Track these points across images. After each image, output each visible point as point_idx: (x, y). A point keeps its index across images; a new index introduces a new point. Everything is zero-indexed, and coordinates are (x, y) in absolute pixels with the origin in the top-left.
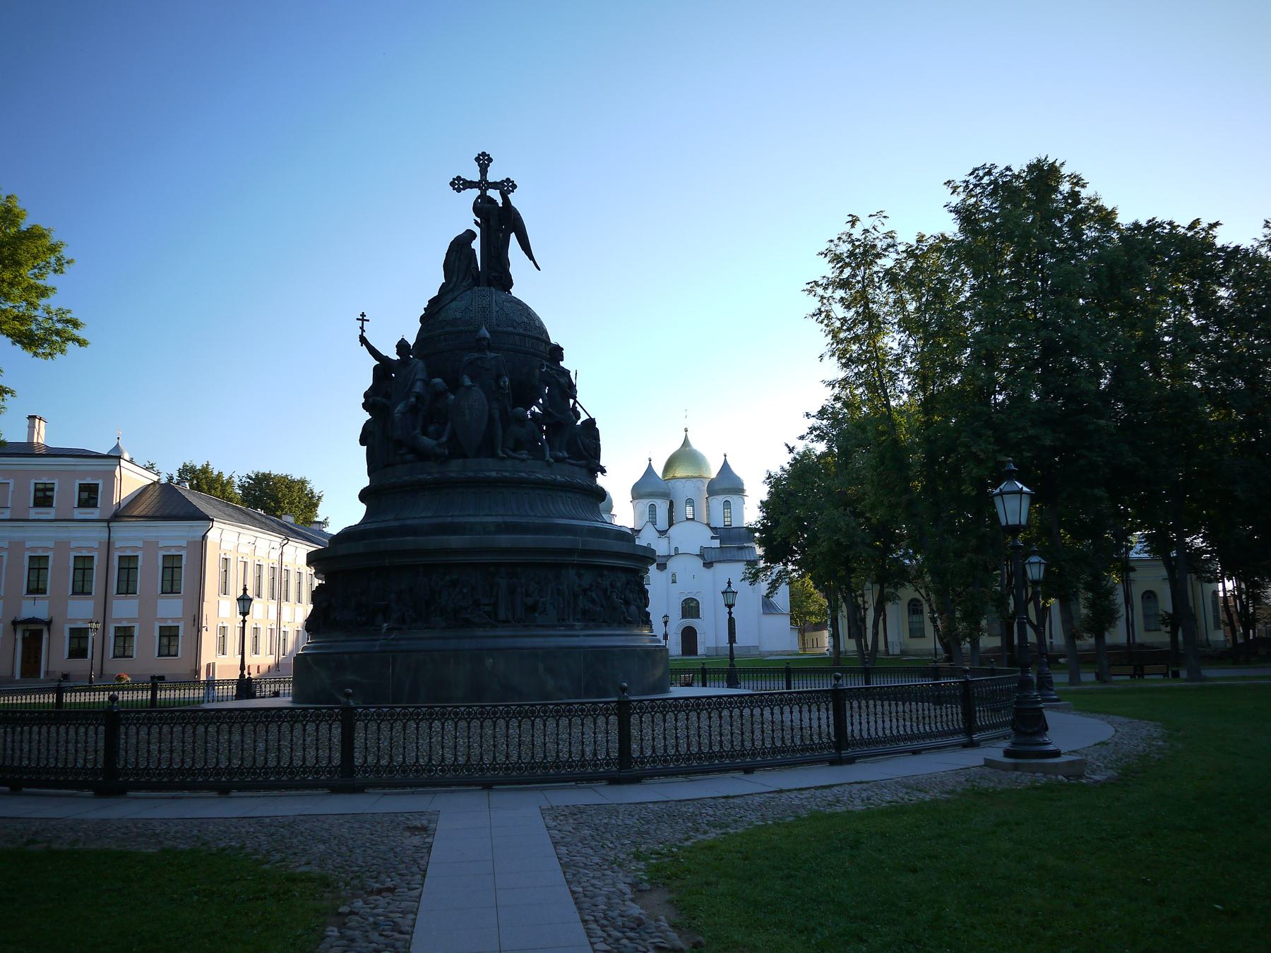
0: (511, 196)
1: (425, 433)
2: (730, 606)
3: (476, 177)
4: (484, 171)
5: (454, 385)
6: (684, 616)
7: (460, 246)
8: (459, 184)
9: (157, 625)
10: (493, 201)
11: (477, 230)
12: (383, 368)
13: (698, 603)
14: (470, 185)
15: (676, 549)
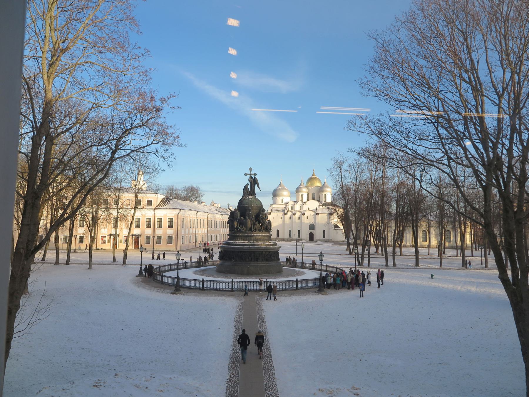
0: (256, 177)
1: (240, 226)
2: (303, 248)
3: (249, 173)
4: (251, 172)
5: (245, 218)
6: (310, 230)
7: (246, 187)
8: (246, 174)
9: (167, 236)
10: (252, 178)
11: (249, 183)
12: (232, 213)
13: (314, 225)
14: (248, 174)
15: (309, 208)
